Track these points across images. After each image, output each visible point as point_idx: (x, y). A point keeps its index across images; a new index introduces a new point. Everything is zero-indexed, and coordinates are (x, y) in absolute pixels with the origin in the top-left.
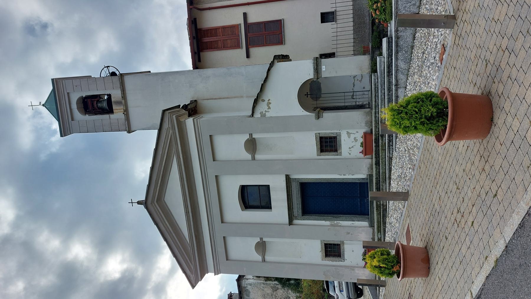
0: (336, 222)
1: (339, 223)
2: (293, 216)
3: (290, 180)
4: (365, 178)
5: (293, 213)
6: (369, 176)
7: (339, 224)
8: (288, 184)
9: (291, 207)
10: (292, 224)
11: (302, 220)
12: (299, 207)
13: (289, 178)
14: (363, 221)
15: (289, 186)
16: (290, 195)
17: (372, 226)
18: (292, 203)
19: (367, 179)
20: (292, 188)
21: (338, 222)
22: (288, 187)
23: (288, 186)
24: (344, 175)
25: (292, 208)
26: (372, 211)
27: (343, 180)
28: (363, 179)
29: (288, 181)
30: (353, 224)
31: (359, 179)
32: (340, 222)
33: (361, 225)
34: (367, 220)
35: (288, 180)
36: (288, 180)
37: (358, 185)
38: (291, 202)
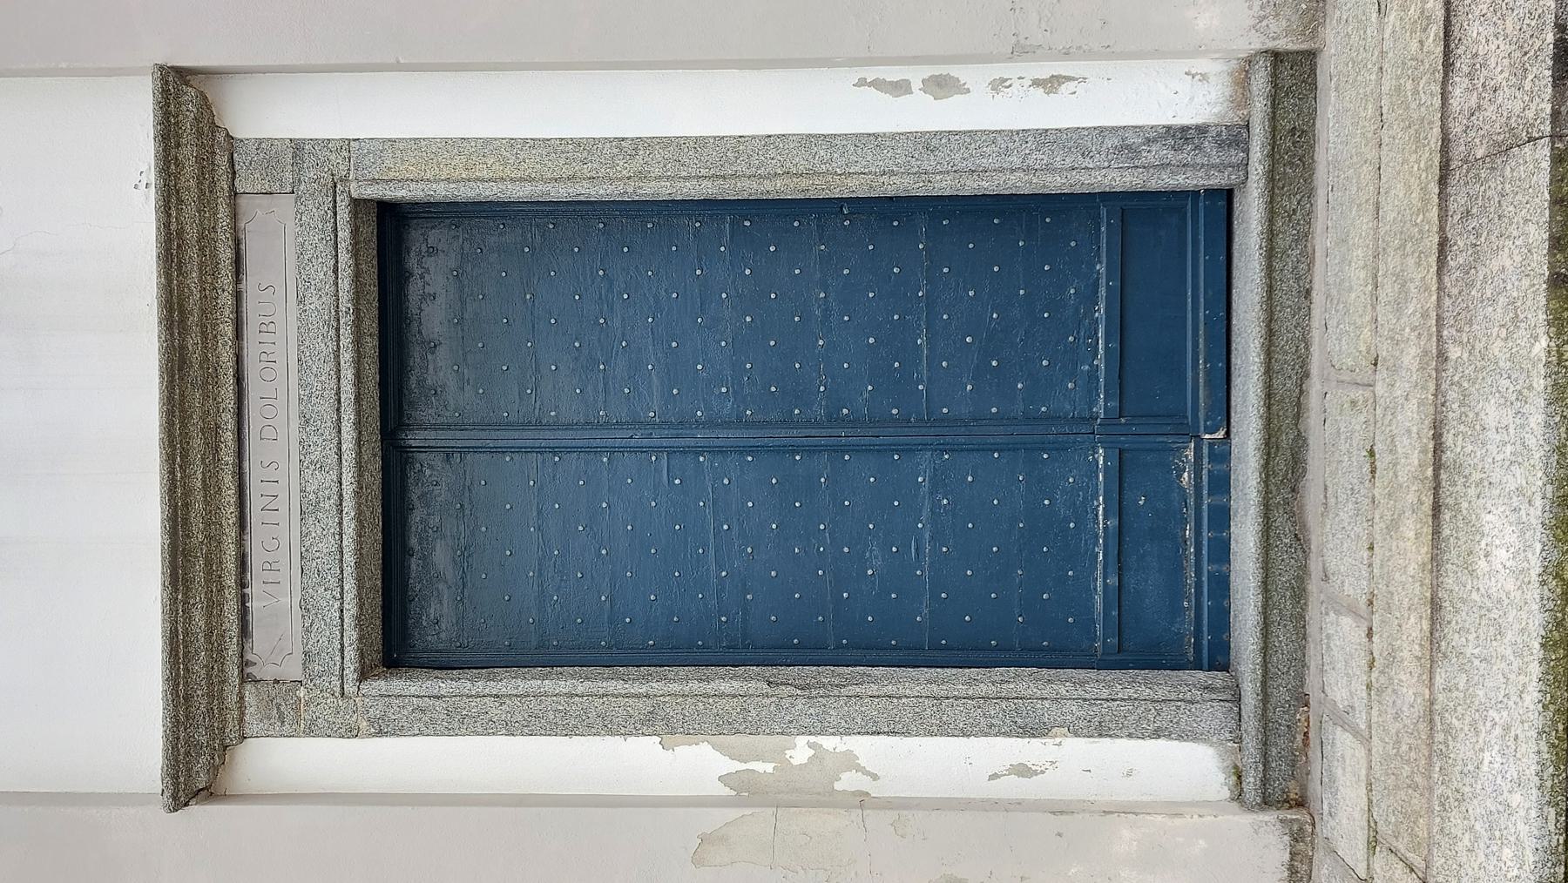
0: (800, 750)
1: (850, 762)
2: (233, 672)
3: (222, 160)
4: (1202, 130)
5: (245, 631)
6: (1260, 82)
7: (848, 782)
8: (190, 210)
9: (214, 540)
10: (209, 793)
11: (353, 733)
12: (329, 544)
13: (209, 126)
14: (1157, 734)
15: (206, 241)
16: (211, 378)
17: (1276, 788)
18: (230, 494)
19: (1236, 137)
20: (250, 284)
21: (829, 742)
22: (193, 253)
23: (192, 233)
24: (941, 86)
25: (230, 565)
26: (1283, 579)
27: (929, 163)
28: (1182, 136)
29: (190, 168)
30: (1023, 771)
31: (1133, 140)
32: (864, 747)
33: (1127, 792)
34: (1213, 713)
35: (188, 153)
36: (188, 153)
37: (1101, 268)
38: (228, 480)
